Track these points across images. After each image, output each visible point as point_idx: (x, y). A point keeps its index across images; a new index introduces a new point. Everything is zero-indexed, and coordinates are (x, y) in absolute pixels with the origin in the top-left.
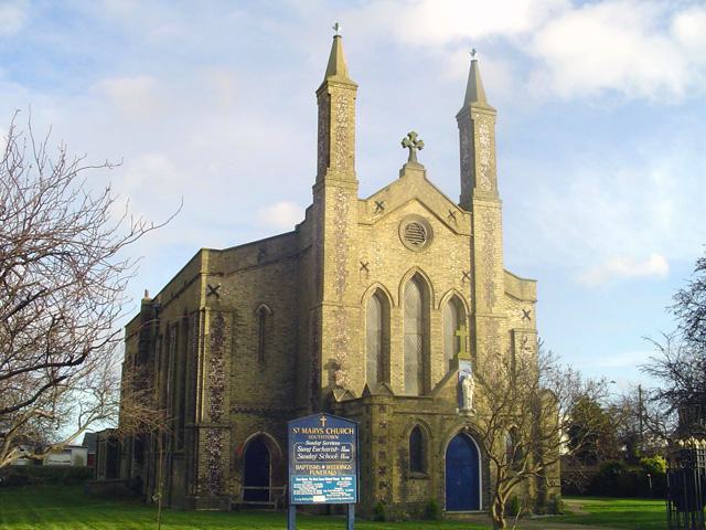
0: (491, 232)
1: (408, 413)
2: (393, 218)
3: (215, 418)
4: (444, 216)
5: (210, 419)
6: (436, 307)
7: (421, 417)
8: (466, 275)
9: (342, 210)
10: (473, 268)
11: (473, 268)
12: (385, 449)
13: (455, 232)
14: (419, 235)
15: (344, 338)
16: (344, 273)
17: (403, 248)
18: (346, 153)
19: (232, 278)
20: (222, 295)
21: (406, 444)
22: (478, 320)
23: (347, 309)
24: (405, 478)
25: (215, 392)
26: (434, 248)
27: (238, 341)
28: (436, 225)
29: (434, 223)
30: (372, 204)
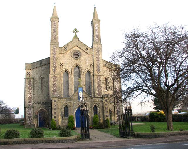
0: (98, 53)
1: (63, 102)
2: (70, 51)
3: (30, 105)
4: (85, 49)
5: (28, 105)
6: (82, 74)
7: (67, 103)
8: (91, 65)
9: (55, 51)
10: (93, 63)
11: (93, 63)
12: (56, 111)
13: (88, 54)
14: (77, 55)
15: (55, 83)
16: (55, 67)
17: (72, 59)
18: (56, 36)
19: (33, 70)
20: (31, 75)
21: (63, 110)
22: (94, 76)
23: (56, 76)
24: (63, 119)
25: (29, 99)
26: (82, 58)
27: (35, 86)
28: (82, 52)
29: (82, 52)
30: (63, 48)
